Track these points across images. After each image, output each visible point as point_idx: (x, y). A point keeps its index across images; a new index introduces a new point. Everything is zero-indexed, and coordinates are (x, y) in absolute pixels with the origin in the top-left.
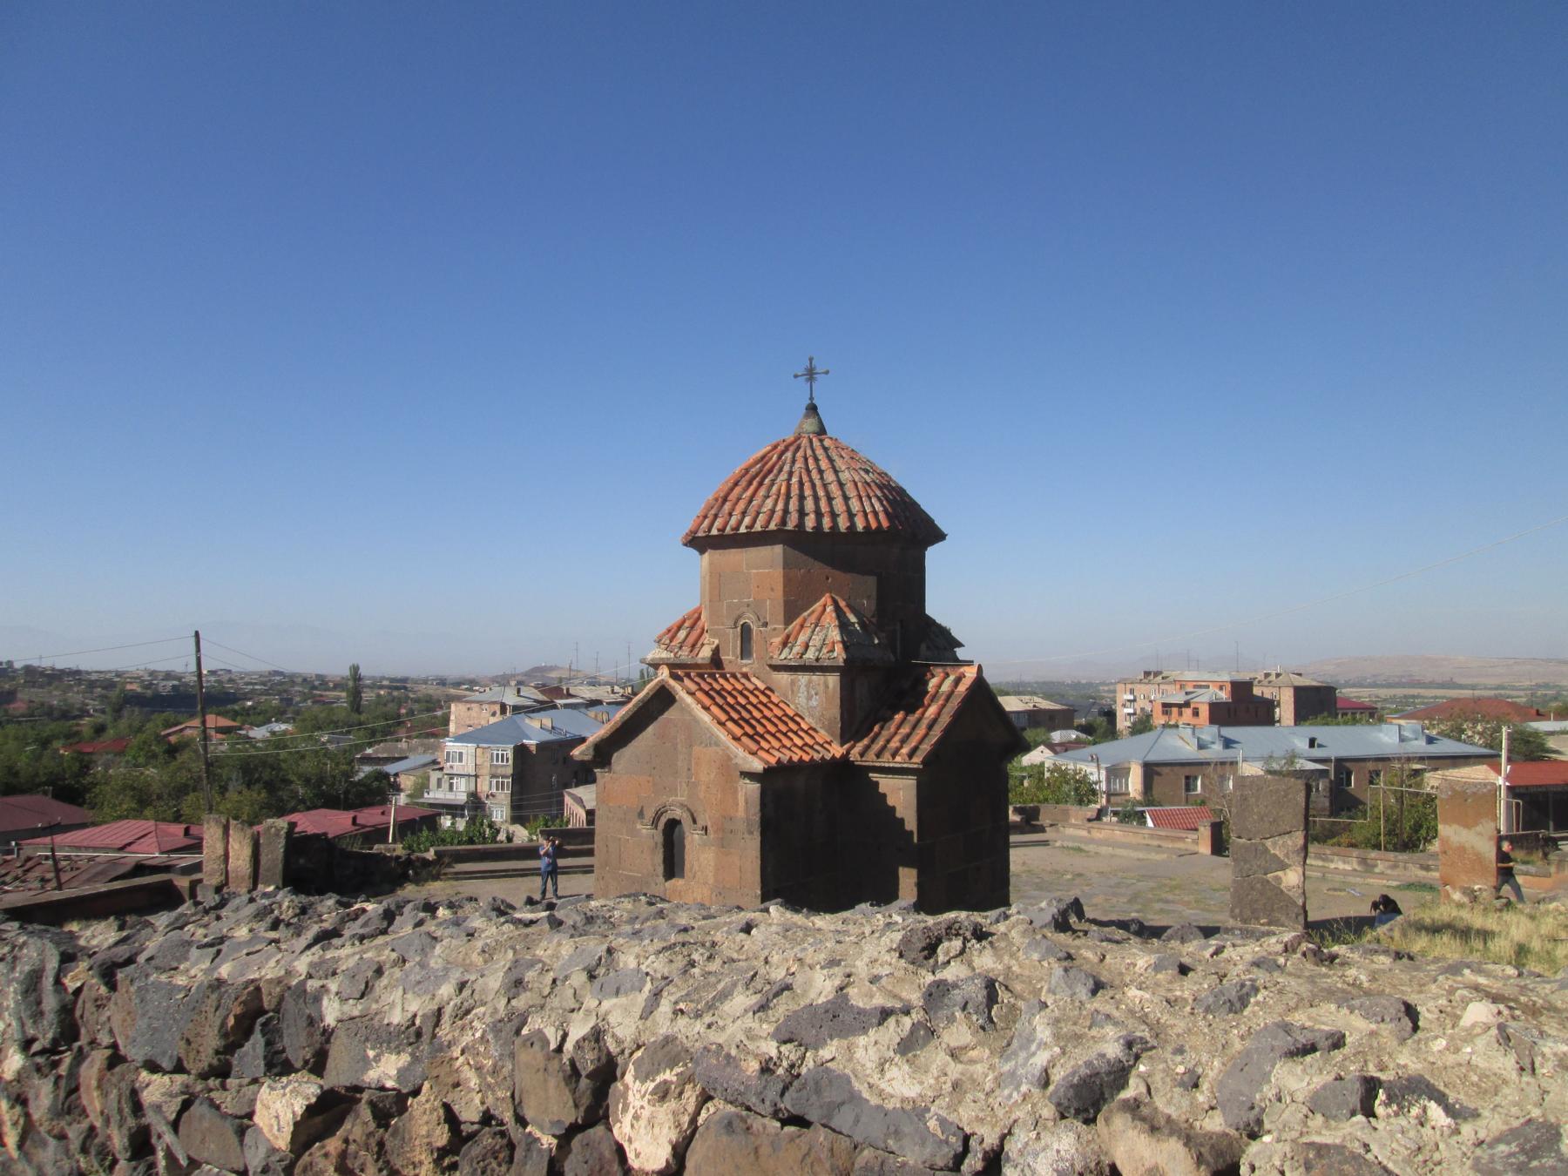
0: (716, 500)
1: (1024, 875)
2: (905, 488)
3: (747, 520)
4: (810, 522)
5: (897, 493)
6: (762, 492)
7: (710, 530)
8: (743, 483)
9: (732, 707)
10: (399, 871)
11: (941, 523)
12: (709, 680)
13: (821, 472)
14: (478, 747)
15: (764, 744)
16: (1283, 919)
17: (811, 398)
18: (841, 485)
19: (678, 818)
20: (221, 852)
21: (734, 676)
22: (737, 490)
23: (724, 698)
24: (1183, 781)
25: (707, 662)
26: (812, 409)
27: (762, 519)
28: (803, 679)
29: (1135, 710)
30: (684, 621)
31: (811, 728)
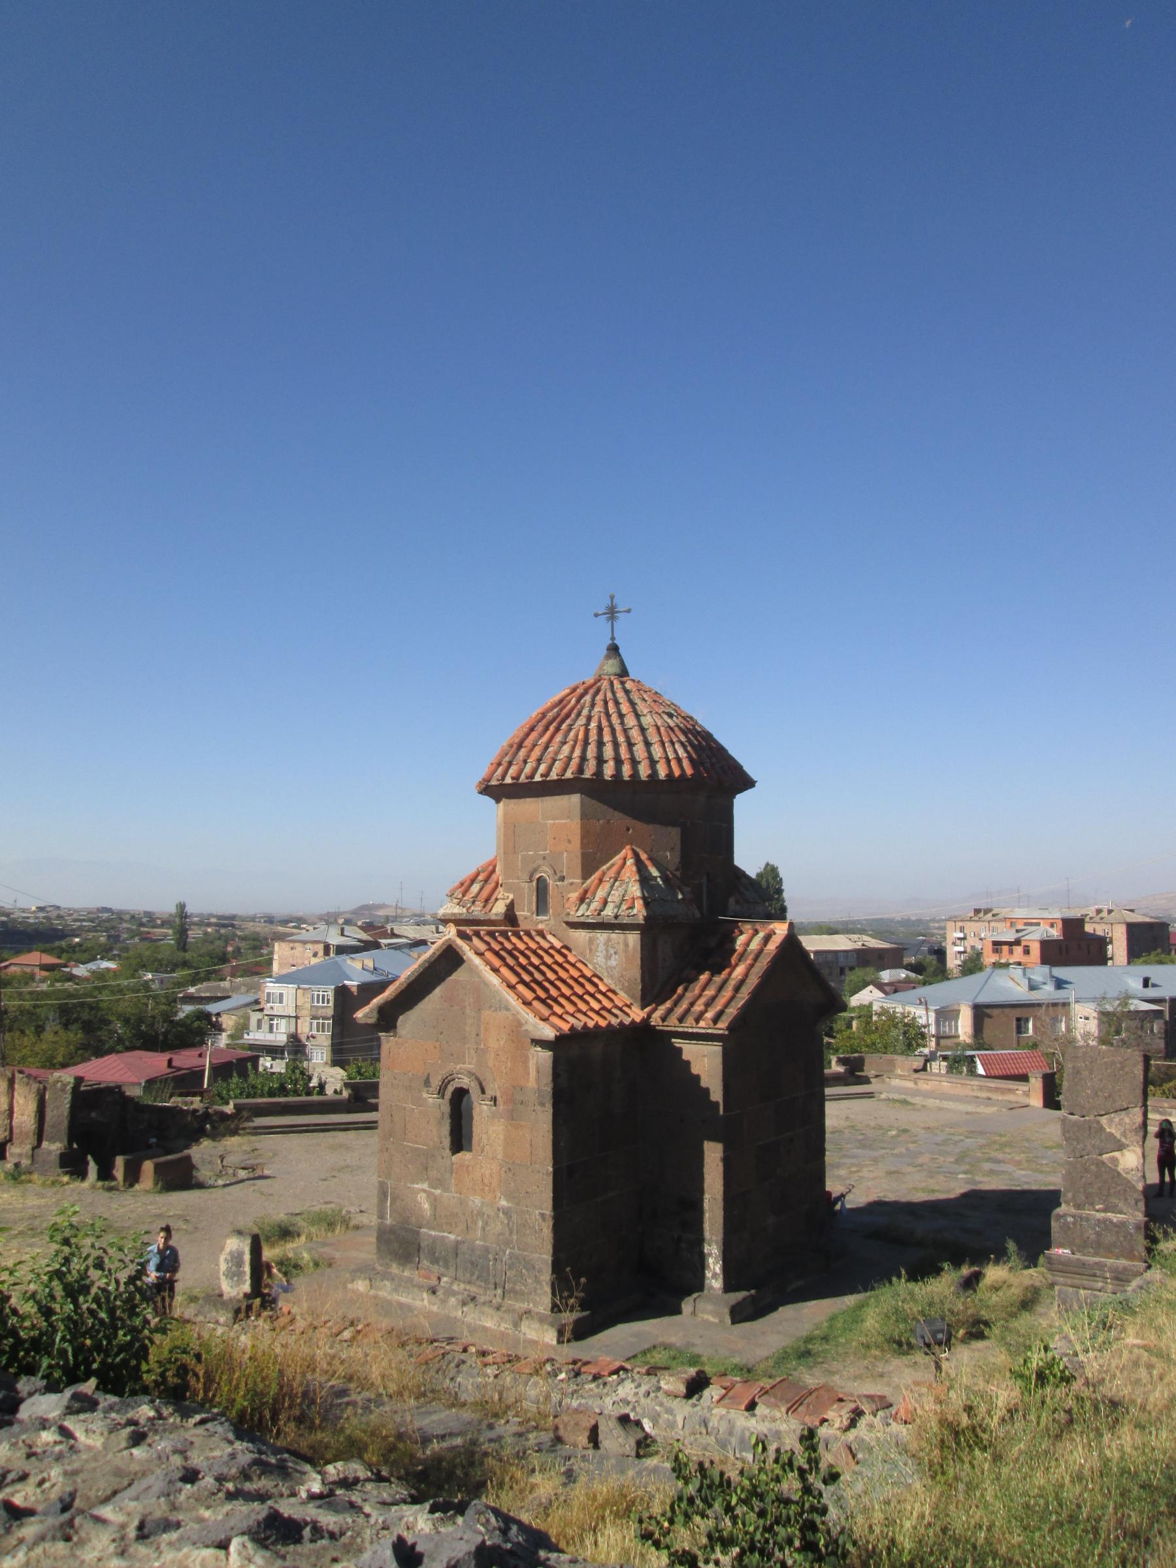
0: (511, 746)
2: (711, 731)
3: (542, 768)
4: (609, 770)
6: (559, 738)
7: (503, 778)
8: (540, 728)
9: (524, 968)
10: (196, 1125)
12: (500, 939)
13: (621, 716)
14: (299, 988)
16: (1121, 1205)
17: (613, 638)
18: (643, 730)
19: (465, 1087)
20: (5, 1106)
21: (528, 934)
22: (534, 735)
23: (516, 958)
24: (1014, 1022)
25: (501, 918)
26: (614, 650)
27: (558, 765)
28: (601, 936)
29: (965, 947)
30: (478, 874)
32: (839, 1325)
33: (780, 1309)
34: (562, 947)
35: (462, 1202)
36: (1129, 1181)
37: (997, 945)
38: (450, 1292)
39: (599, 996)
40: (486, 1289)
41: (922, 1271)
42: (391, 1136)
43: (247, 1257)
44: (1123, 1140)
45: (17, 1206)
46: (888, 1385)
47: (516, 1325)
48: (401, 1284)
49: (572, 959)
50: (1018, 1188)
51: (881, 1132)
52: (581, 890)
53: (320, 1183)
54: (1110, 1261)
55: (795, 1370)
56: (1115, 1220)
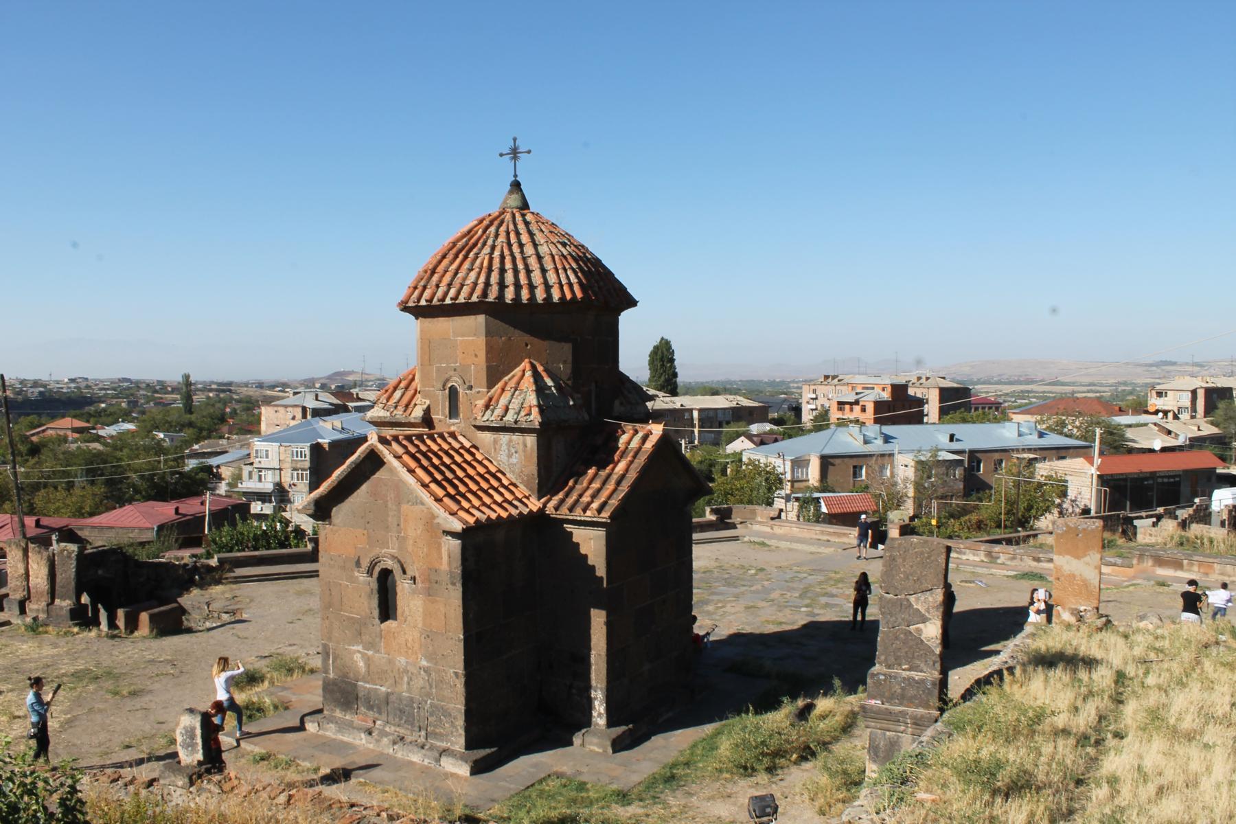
0: (426, 272)
2: (600, 257)
3: (452, 292)
4: (509, 294)
6: (466, 265)
7: (419, 300)
8: (450, 256)
10: (186, 577)
11: (632, 291)
12: (416, 442)
13: (521, 246)
15: (465, 504)
17: (515, 176)
18: (540, 258)
20: (22, 571)
21: (442, 436)
22: (446, 262)
23: (429, 459)
25: (418, 421)
26: (516, 186)
27: (465, 290)
28: (504, 438)
29: (816, 406)
31: (512, 484)
33: (653, 738)
34: (471, 447)
35: (391, 662)
37: (841, 404)
38: (383, 734)
40: (412, 731)
41: (768, 704)
42: (330, 607)
43: (198, 732)
44: (927, 614)
45: (33, 656)
46: (734, 804)
47: (438, 760)
49: (479, 457)
52: (486, 398)
55: (662, 793)
56: (917, 678)
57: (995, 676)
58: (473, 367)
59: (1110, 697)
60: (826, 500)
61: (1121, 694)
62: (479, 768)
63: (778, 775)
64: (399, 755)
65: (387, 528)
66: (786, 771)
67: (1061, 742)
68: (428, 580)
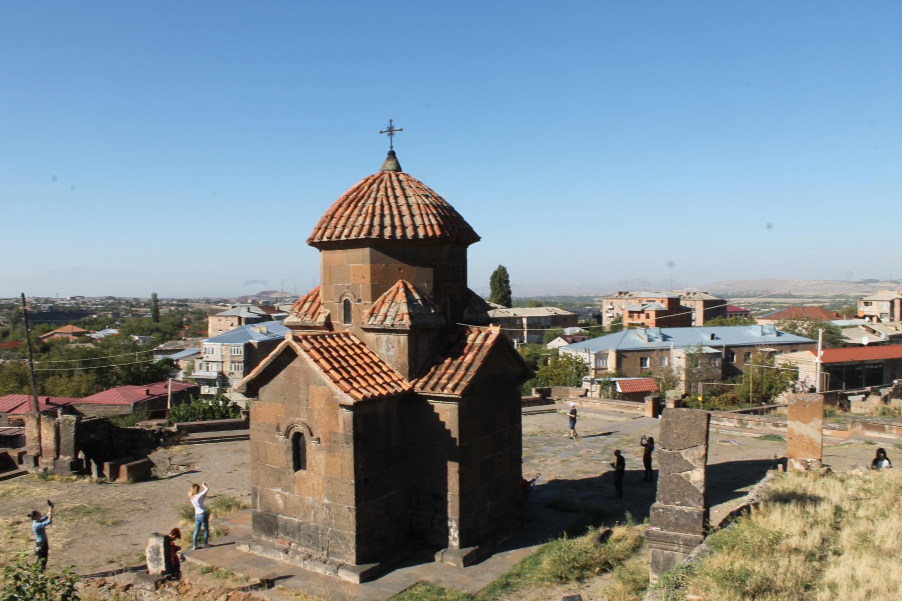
0: (327, 217)
1: (539, 434)
3: (346, 231)
4: (387, 233)
5: (447, 210)
6: (356, 212)
7: (322, 238)
8: (345, 206)
10: (154, 439)
12: (320, 340)
13: (396, 197)
15: (356, 385)
16: (690, 501)
17: (392, 147)
18: (409, 206)
19: (301, 432)
20: (36, 435)
21: (338, 336)
22: (341, 210)
23: (330, 353)
25: (322, 325)
26: (392, 154)
27: (356, 230)
28: (384, 337)
30: (308, 297)
32: (527, 566)
33: (493, 556)
34: (360, 343)
35: (301, 500)
36: (696, 488)
37: (631, 313)
38: (296, 553)
39: (382, 375)
41: (577, 531)
42: (258, 460)
43: (162, 550)
44: (693, 464)
45: (44, 496)
47: (336, 572)
48: (268, 547)
49: (366, 351)
50: (636, 469)
51: (560, 434)
52: (371, 308)
53: (228, 474)
54: (682, 534)
55: (500, 596)
56: (686, 511)
57: (744, 510)
58: (361, 286)
59: (831, 525)
60: (621, 382)
61: (839, 523)
62: (366, 578)
63: (585, 583)
64: (308, 568)
65: (299, 403)
66: (591, 580)
67: (793, 558)
68: (328, 440)
